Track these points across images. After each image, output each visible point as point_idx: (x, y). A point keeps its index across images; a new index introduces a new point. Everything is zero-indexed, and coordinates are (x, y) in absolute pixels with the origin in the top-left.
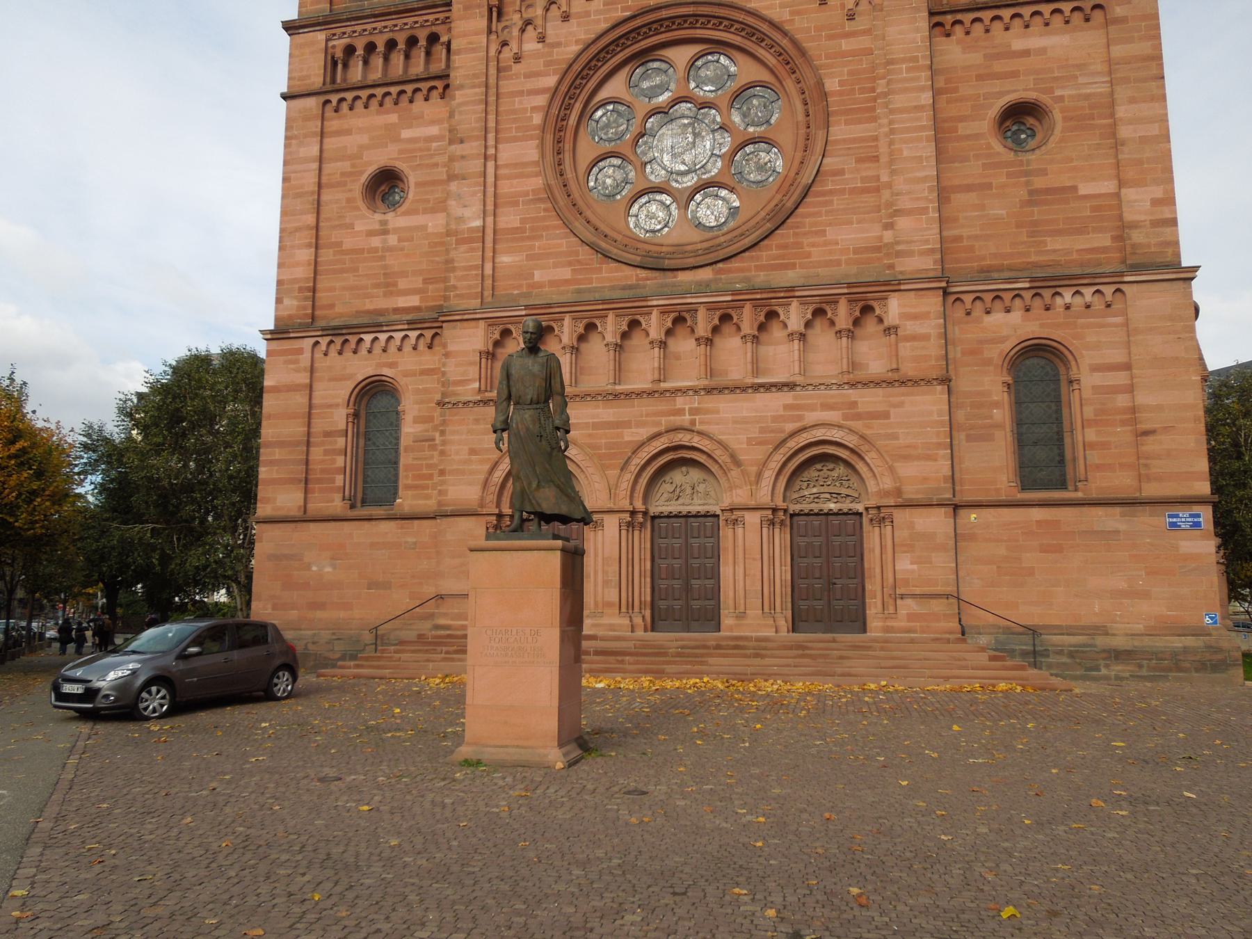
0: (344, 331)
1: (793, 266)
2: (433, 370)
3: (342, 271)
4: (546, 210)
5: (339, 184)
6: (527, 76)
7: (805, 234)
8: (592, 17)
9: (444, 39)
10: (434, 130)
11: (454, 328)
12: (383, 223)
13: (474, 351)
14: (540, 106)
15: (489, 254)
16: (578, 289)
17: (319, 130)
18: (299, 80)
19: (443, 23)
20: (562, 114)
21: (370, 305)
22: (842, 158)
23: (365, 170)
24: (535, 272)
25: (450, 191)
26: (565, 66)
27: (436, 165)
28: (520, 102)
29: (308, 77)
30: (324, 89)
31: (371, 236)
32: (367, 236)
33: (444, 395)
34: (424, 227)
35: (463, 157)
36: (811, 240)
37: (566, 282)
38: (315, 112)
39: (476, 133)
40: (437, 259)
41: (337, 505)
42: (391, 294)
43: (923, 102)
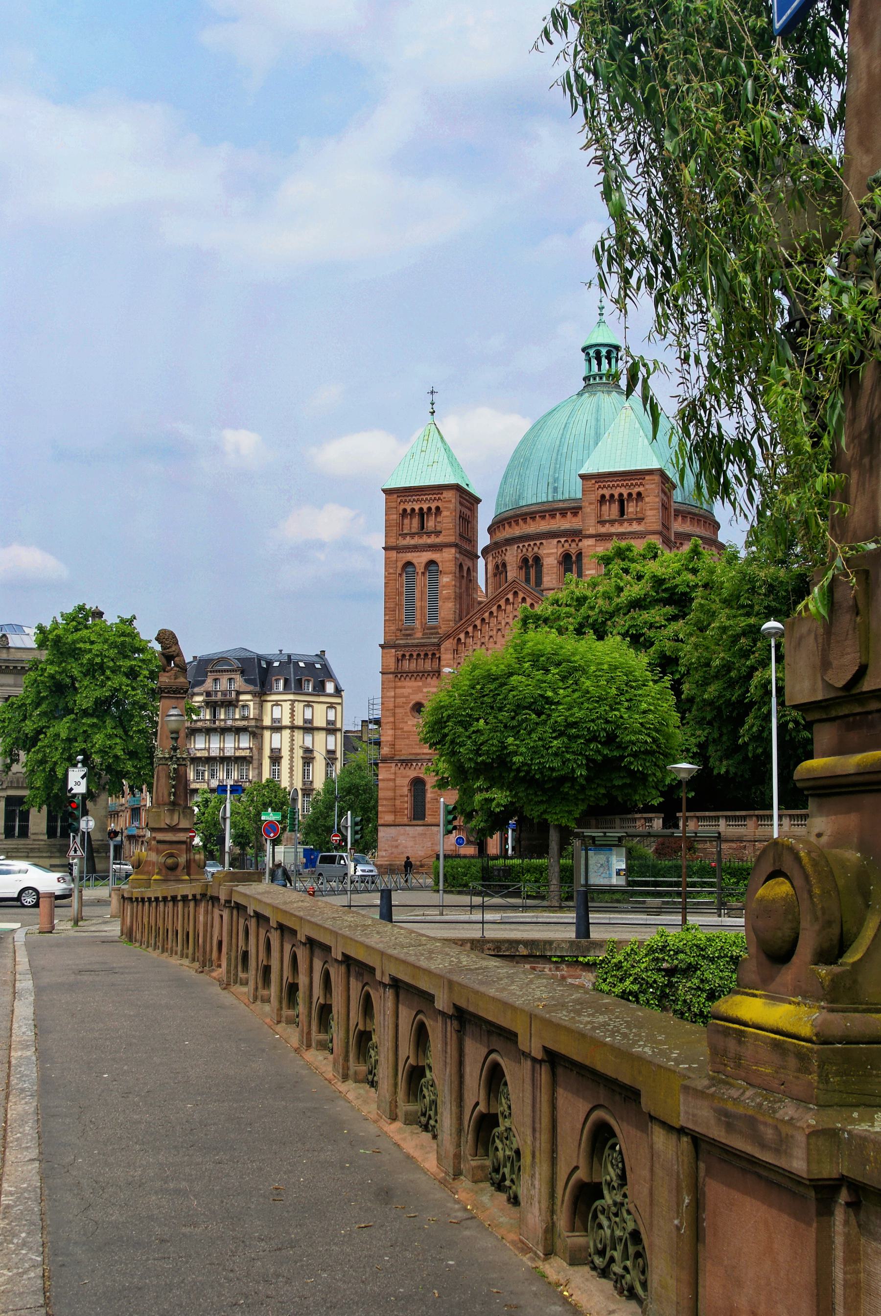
21: (414, 751)
41: (405, 820)
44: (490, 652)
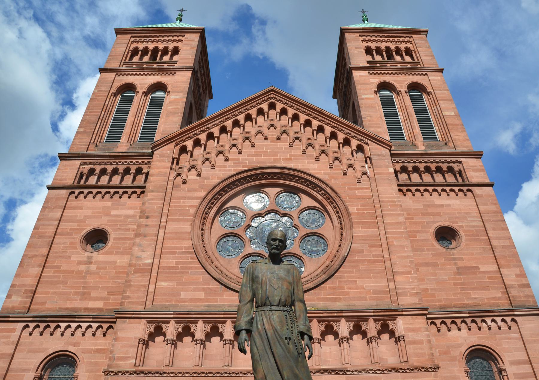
0: (48, 319)
1: (340, 299)
2: (104, 350)
3: (56, 283)
4: (191, 258)
5: (68, 234)
6: (188, 190)
7: (345, 282)
8: (227, 168)
9: (145, 171)
10: (131, 212)
11: (124, 322)
12: (90, 258)
13: (135, 338)
14: (195, 205)
15: (153, 279)
16: (208, 305)
17: (64, 205)
18: (59, 181)
19: (146, 164)
20: (206, 210)
21: (69, 305)
22: (361, 245)
23: (86, 229)
24: (181, 293)
25: (136, 242)
26: (210, 188)
27: (129, 230)
28: (183, 202)
29: (65, 179)
30: (73, 186)
31: (80, 264)
32: (78, 264)
33: (109, 366)
34: (115, 262)
35: (147, 225)
36: (348, 286)
37: (200, 300)
38: (64, 196)
39: (156, 214)
40: (119, 281)
42: (85, 299)
43: (400, 221)
44: (230, 163)
